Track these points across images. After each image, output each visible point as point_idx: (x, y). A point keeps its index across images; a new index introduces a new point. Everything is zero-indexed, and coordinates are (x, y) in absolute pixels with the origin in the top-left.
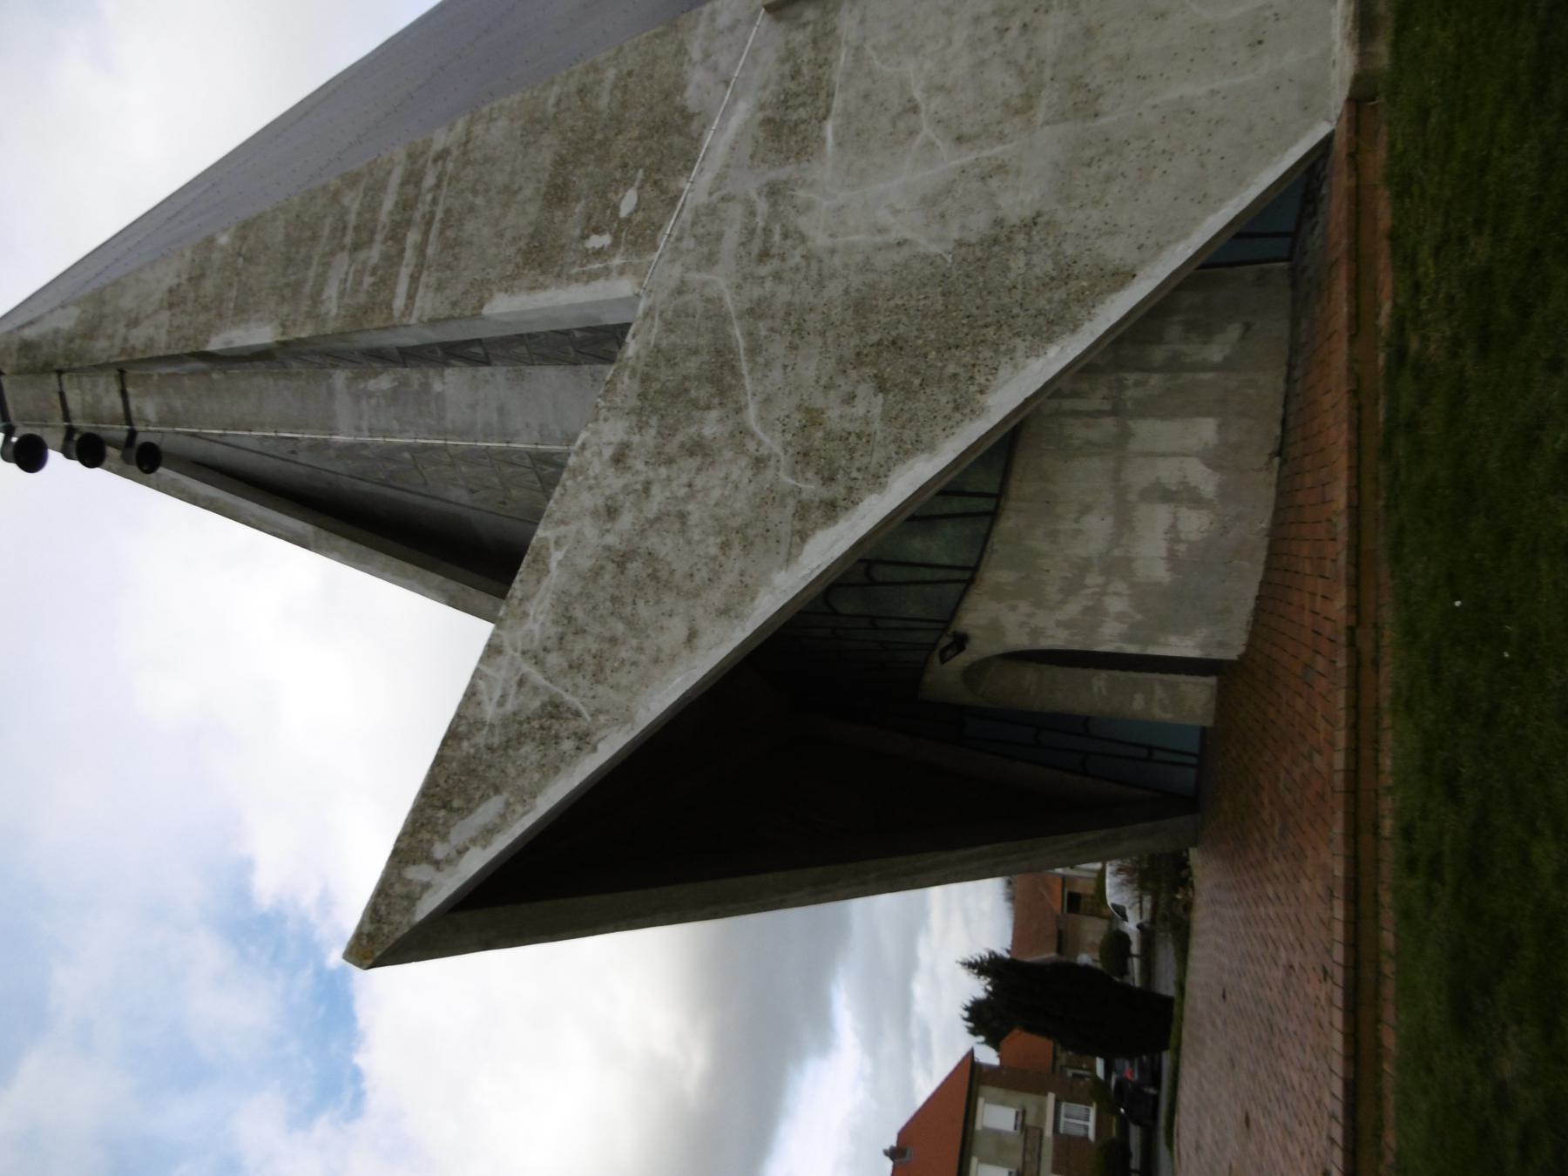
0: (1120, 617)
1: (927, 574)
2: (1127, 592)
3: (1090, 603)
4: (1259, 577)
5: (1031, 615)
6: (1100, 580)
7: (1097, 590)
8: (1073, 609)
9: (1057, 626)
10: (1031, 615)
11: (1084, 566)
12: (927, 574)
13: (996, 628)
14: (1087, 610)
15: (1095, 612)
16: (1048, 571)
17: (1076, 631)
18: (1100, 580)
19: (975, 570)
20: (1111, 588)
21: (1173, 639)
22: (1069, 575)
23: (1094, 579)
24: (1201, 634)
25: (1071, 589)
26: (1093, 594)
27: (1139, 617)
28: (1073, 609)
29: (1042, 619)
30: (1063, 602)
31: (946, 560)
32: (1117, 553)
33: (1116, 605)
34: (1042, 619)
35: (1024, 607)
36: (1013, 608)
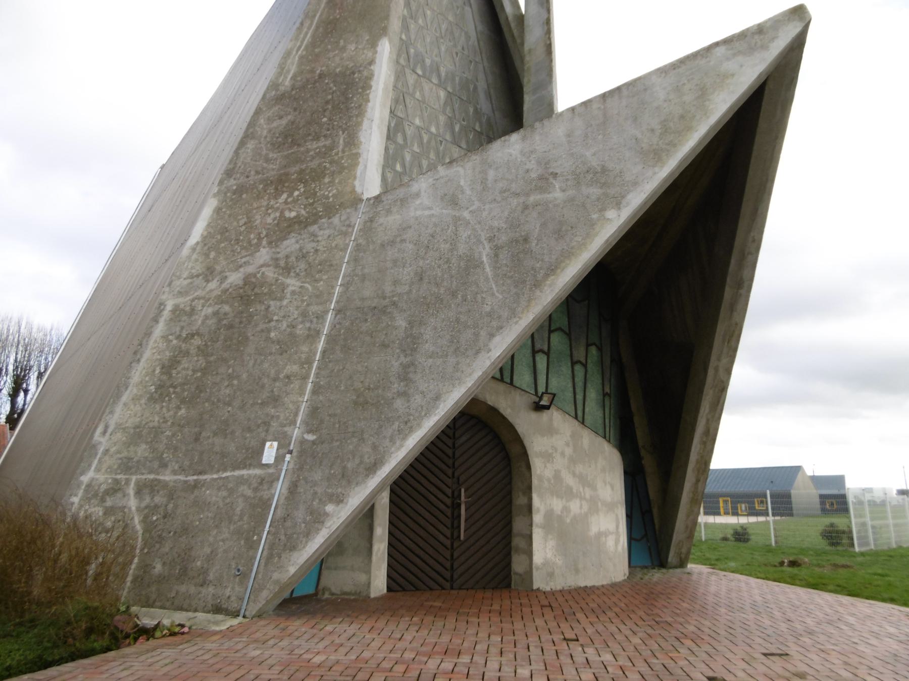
0: (566, 509)
1: (580, 397)
2: (583, 512)
3: (575, 491)
4: (596, 584)
5: (563, 454)
6: (588, 496)
7: (583, 494)
8: (569, 480)
9: (555, 471)
10: (563, 454)
11: (594, 488)
12: (580, 397)
13: (550, 431)
14: (570, 489)
15: (569, 494)
16: (590, 467)
17: (552, 482)
18: (588, 496)
19: (583, 423)
20: (584, 503)
21: (551, 543)
22: (589, 479)
23: (588, 493)
24: (559, 561)
25: (583, 480)
26: (580, 493)
27: (568, 521)
28: (569, 480)
29: (560, 463)
30: (574, 475)
31: (587, 410)
32: (600, 504)
33: (575, 507)
34: (560, 463)
35: (569, 451)
36: (567, 445)
